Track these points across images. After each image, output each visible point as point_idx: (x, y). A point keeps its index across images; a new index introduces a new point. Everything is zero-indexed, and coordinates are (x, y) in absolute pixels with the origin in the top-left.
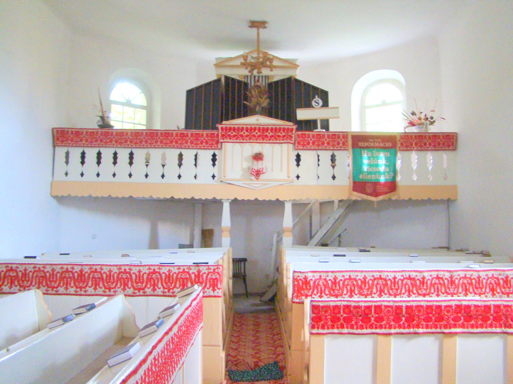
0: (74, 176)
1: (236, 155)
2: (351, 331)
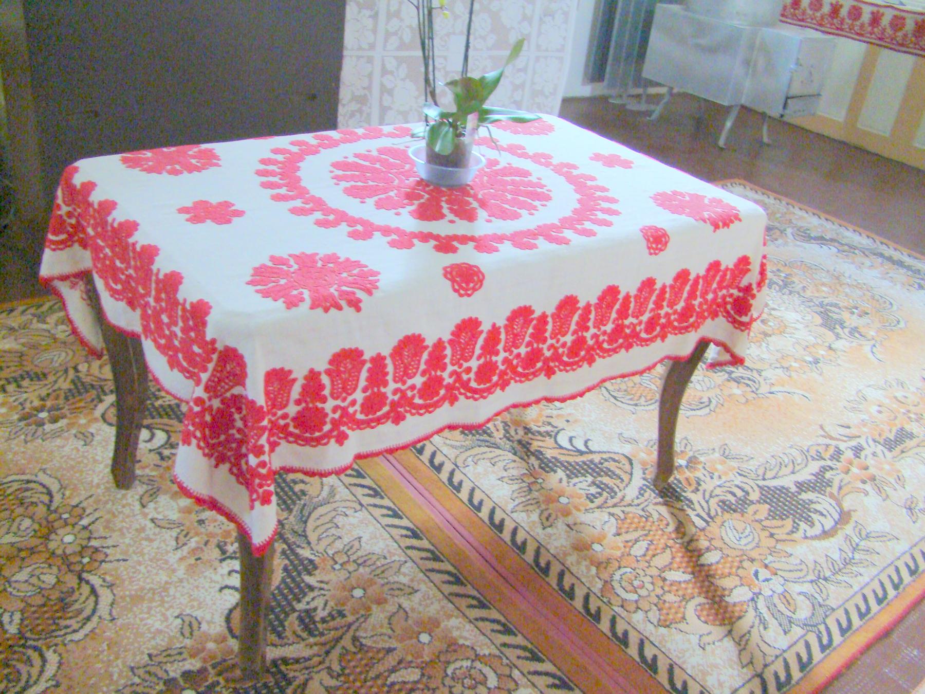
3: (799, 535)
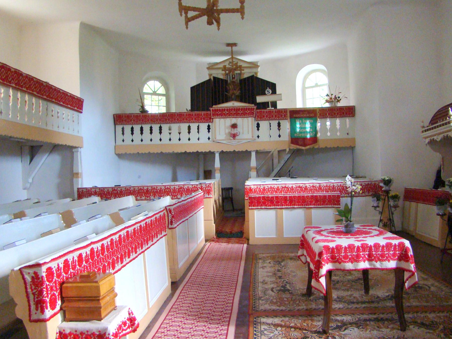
0: (128, 142)
1: (221, 125)
2: (266, 207)
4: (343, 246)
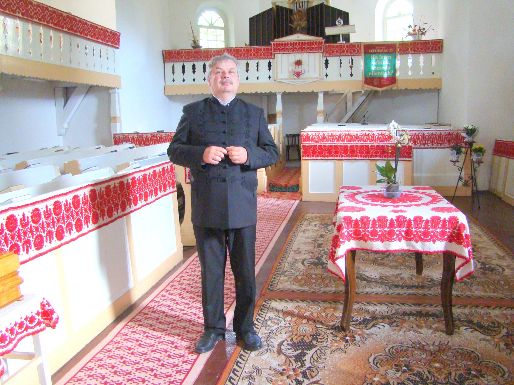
1: (284, 62)
3: (289, 340)
4: (371, 219)
